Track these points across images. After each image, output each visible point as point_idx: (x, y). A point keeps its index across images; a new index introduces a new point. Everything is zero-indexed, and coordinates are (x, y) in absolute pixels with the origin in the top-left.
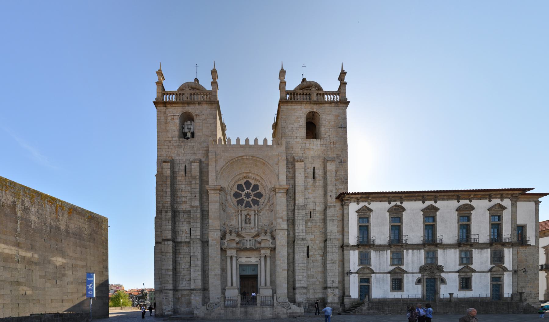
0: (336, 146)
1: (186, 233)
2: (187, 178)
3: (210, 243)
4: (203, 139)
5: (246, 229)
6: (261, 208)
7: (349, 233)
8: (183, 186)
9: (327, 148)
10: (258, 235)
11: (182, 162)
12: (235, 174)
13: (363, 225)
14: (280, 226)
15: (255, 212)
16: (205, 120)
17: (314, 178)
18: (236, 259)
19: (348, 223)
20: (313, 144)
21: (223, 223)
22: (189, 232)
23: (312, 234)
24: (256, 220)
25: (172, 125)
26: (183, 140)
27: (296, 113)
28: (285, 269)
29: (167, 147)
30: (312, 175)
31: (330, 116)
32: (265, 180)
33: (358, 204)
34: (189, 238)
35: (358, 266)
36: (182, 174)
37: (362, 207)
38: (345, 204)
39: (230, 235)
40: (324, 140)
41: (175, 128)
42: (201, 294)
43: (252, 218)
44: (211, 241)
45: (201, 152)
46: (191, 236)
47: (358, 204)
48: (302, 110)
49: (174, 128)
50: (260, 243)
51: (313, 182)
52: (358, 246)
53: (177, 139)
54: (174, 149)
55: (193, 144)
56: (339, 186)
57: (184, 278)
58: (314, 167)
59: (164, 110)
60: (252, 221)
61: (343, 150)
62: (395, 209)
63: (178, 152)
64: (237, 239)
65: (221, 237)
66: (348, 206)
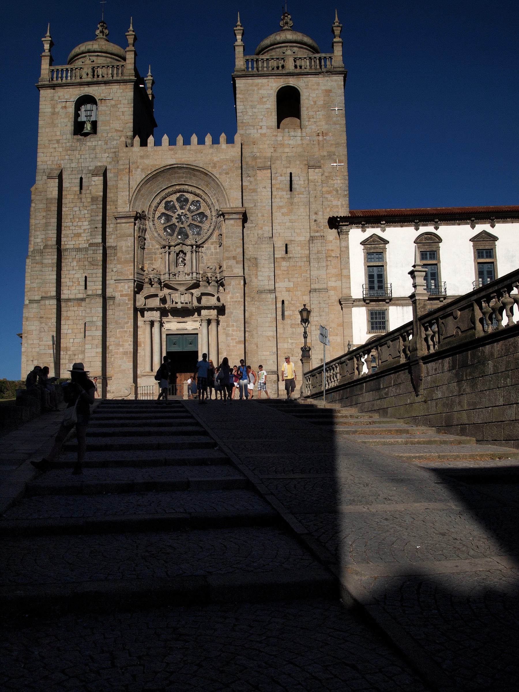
0: (328, 138)
1: (79, 284)
2: (83, 196)
3: (117, 301)
4: (109, 135)
5: (177, 275)
6: (203, 240)
7: (350, 278)
9: (312, 142)
10: (196, 286)
11: (76, 172)
12: (161, 188)
13: (375, 265)
14: (232, 271)
15: (193, 248)
16: (113, 106)
17: (291, 190)
18: (160, 325)
19: (348, 263)
20: (289, 136)
21: (140, 267)
22: (83, 283)
23: (289, 282)
24: (194, 261)
26: (79, 138)
27: (261, 90)
29: (52, 150)
30: (288, 186)
31: (317, 92)
32: (210, 196)
33: (364, 231)
34: (84, 291)
35: (367, 334)
37: (371, 237)
38: (341, 232)
39: (150, 286)
40: (307, 130)
41: (67, 121)
43: (188, 255)
44: (119, 297)
45: (107, 155)
46: (86, 288)
47: (364, 231)
48: (270, 84)
49: (66, 120)
50: (199, 300)
51: (289, 196)
52: (365, 301)
53: (69, 136)
54: (64, 153)
56: (333, 202)
57: (72, 360)
58: (291, 174)
61: (338, 144)
62: (426, 238)
63: (70, 156)
64: (161, 294)
66: (347, 233)
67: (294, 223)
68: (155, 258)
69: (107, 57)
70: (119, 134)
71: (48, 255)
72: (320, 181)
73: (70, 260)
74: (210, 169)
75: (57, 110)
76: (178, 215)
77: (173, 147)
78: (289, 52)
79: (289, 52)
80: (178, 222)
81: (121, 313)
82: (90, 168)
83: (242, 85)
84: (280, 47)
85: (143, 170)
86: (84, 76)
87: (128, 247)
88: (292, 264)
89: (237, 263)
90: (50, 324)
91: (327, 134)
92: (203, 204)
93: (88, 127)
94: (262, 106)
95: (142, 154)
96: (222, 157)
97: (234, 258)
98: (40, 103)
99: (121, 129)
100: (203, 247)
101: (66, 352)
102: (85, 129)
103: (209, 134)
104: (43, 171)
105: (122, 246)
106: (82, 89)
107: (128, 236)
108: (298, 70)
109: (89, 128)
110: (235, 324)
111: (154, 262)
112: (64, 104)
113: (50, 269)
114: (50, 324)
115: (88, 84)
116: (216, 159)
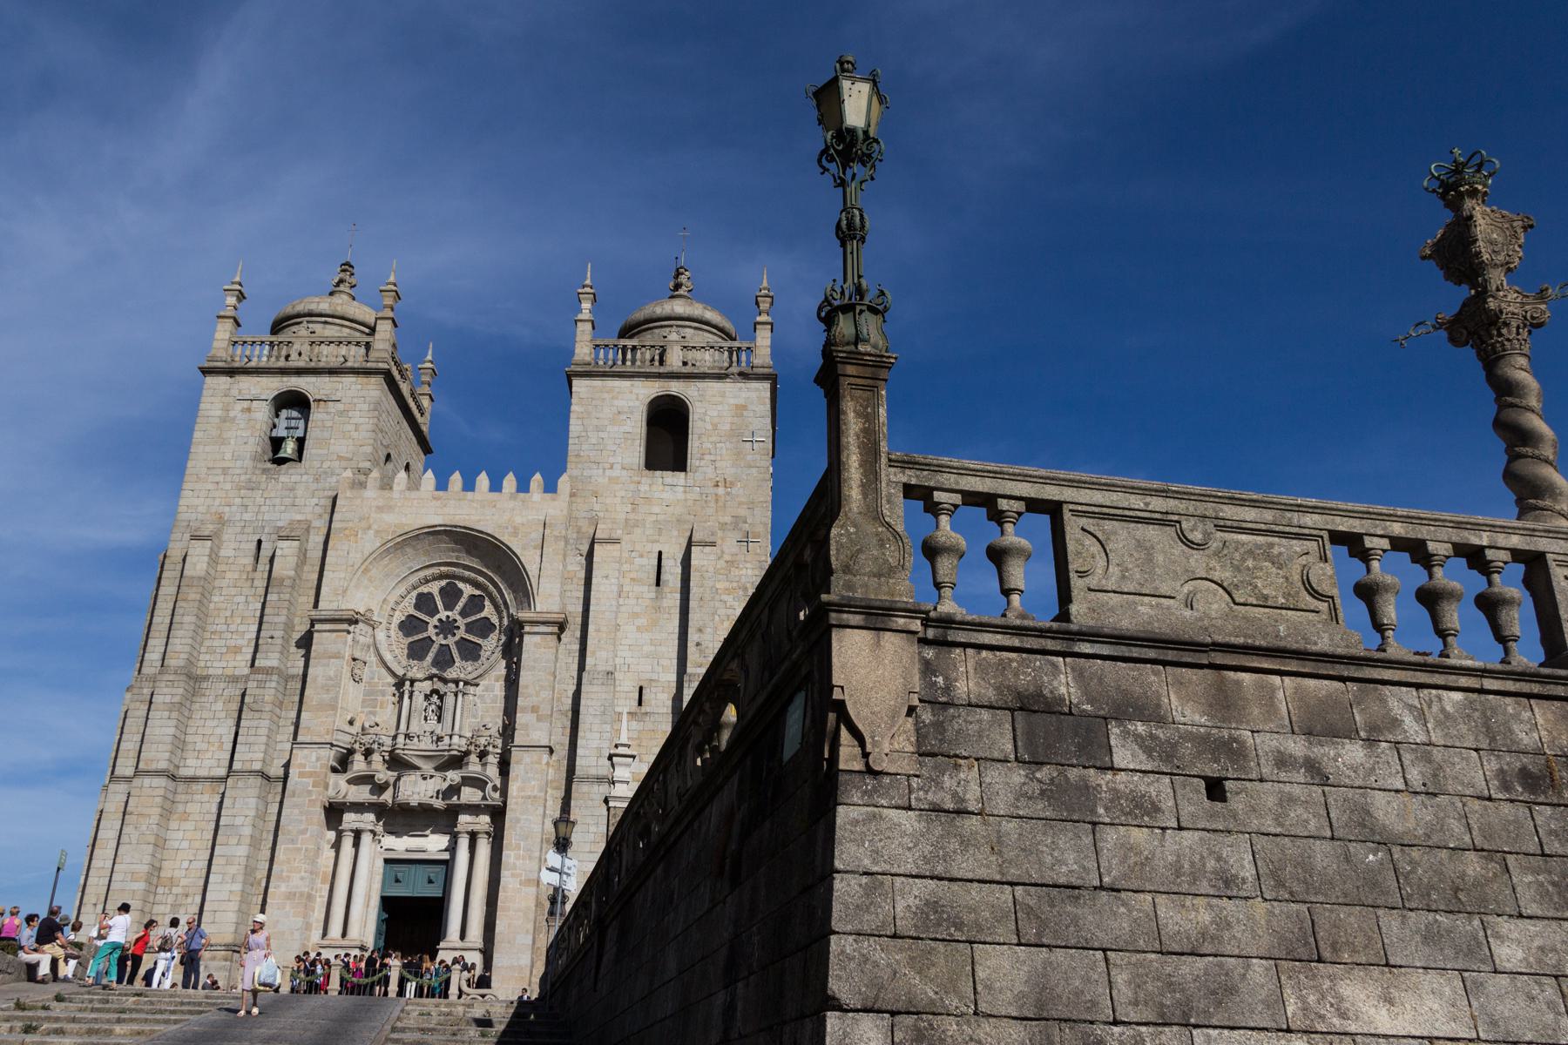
0: (734, 491)
1: (221, 747)
4: (326, 465)
6: (480, 671)
8: (242, 599)
14: (528, 735)
16: (341, 413)
21: (349, 718)
25: (242, 426)
27: (617, 398)
28: (529, 880)
29: (210, 486)
31: (720, 408)
36: (244, 565)
40: (697, 474)
42: (228, 963)
43: (449, 699)
45: (315, 501)
51: (653, 595)
53: (248, 463)
55: (295, 478)
57: (180, 905)
58: (660, 553)
60: (448, 716)
61: (753, 503)
65: (334, 764)
67: (659, 648)
68: (382, 703)
69: (342, 326)
70: (344, 464)
71: (167, 686)
72: (711, 569)
73: (211, 699)
74: (505, 539)
75: (232, 414)
76: (440, 620)
77: (441, 493)
78: (674, 336)
79: (674, 336)
80: (437, 634)
81: (296, 811)
82: (280, 524)
83: (583, 389)
84: (662, 327)
85: (377, 532)
86: (294, 356)
87: (331, 679)
88: (649, 726)
89: (539, 719)
90: (144, 827)
91: (732, 484)
92: (487, 603)
93: (289, 448)
94: (616, 429)
95: (380, 504)
96: (530, 517)
97: (534, 709)
98: (203, 399)
99: (350, 456)
100: (477, 685)
101: (170, 890)
102: (282, 451)
103: (511, 474)
104: (185, 524)
105: (317, 676)
106: (285, 379)
107: (330, 657)
108: (688, 369)
109: (289, 450)
110: (522, 843)
111: (378, 709)
113: (167, 713)
114: (144, 827)
115: (299, 372)
116: (518, 520)
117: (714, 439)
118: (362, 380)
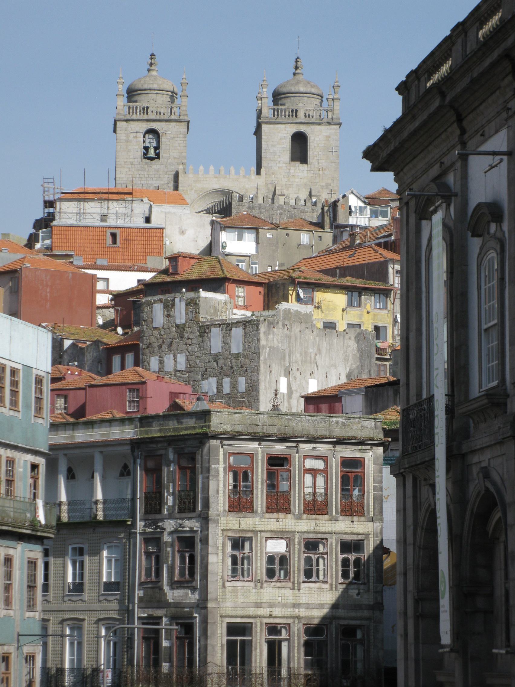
0: (326, 172)
4: (170, 161)
16: (173, 139)
31: (320, 137)
45: (167, 176)
48: (287, 129)
53: (140, 160)
55: (158, 166)
59: (126, 126)
75: (130, 139)
84: (294, 97)
85: (195, 191)
86: (150, 113)
91: (325, 169)
102: (149, 153)
108: (307, 120)
112: (134, 135)
115: (154, 121)
116: (247, 186)
117: (317, 150)
118: (178, 123)
